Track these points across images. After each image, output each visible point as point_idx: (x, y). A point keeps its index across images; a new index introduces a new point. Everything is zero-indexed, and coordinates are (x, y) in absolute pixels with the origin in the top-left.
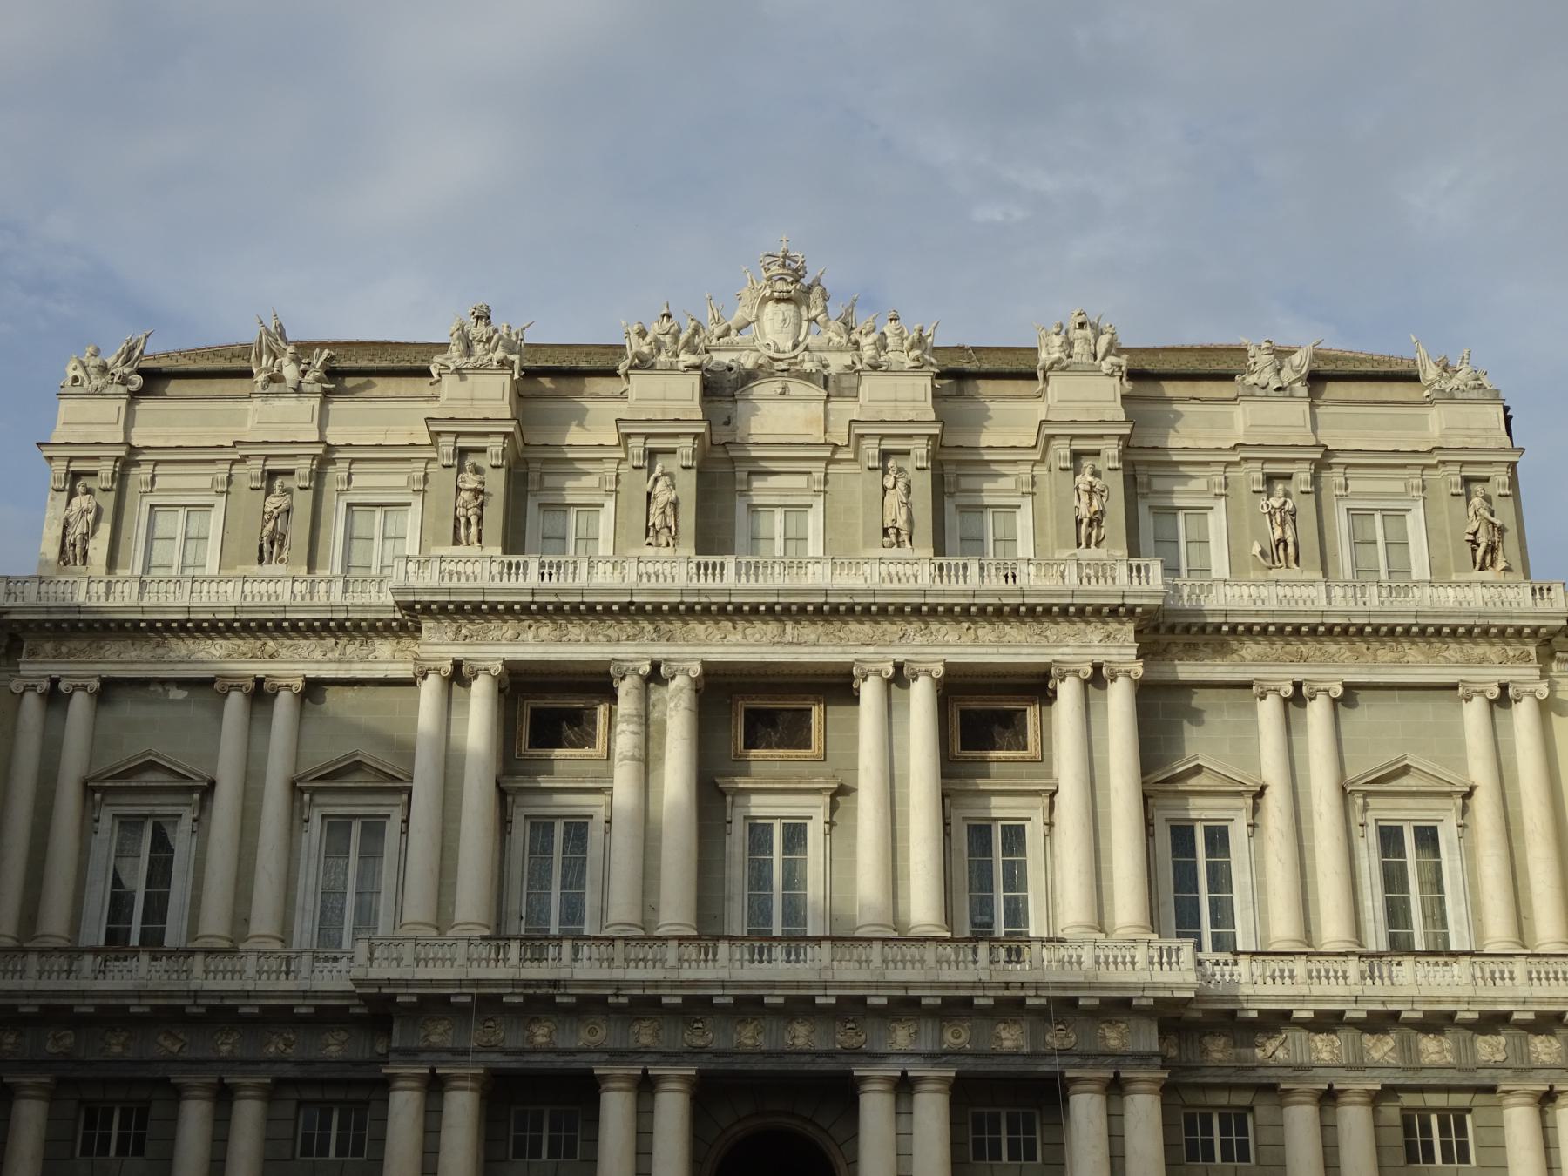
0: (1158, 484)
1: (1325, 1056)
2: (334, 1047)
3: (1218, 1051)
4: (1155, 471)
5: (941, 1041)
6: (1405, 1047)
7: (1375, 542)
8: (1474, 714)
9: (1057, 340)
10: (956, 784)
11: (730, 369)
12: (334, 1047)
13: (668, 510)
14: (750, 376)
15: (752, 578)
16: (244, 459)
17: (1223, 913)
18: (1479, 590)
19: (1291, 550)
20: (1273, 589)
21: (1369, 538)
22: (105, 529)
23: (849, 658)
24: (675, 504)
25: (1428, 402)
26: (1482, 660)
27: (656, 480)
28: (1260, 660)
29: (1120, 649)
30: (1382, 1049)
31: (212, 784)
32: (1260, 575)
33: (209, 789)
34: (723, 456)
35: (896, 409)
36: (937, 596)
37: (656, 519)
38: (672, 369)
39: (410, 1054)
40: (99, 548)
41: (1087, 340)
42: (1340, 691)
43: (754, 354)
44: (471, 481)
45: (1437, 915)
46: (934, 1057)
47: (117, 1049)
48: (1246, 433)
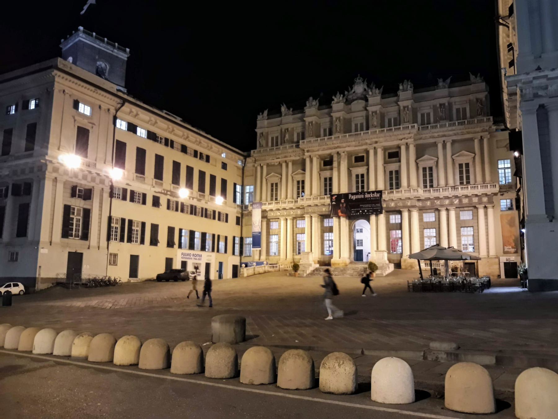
2: (299, 212)
3: (428, 203)
6: (460, 201)
8: (476, 142)
12: (299, 212)
17: (431, 181)
26: (478, 132)
29: (410, 141)
30: (456, 201)
33: (281, 179)
39: (307, 213)
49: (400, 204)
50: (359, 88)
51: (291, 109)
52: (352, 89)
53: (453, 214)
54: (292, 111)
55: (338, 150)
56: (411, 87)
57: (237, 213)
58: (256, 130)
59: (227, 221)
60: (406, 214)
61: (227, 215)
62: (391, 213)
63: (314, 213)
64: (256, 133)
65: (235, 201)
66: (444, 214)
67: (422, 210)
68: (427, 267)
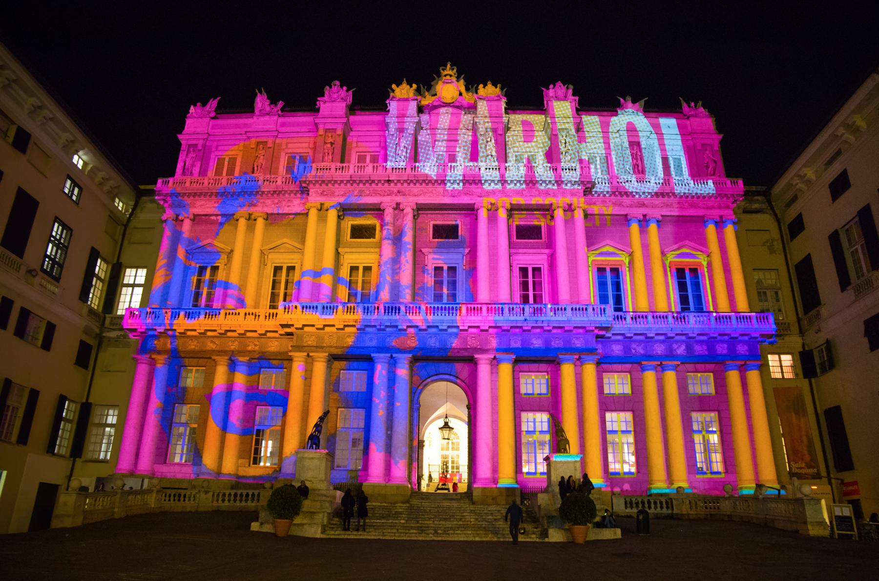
1: (659, 352)
5: (510, 345)
6: (689, 348)
10: (514, 251)
16: (249, 138)
19: (640, 168)
22: (198, 164)
23: (472, 202)
25: (688, 118)
26: (712, 208)
28: (631, 206)
31: (232, 251)
40: (196, 171)
42: (660, 218)
44: (330, 140)
45: (698, 298)
46: (508, 351)
47: (193, 347)
49: (556, 343)
50: (449, 88)
51: (280, 104)
52: (428, 90)
53: (670, 377)
54: (282, 110)
55: (399, 199)
56: (574, 95)
57: (87, 331)
58: (180, 137)
59: (47, 345)
60: (567, 371)
61: (51, 328)
62: (525, 366)
63: (319, 348)
64: (180, 144)
65: (84, 294)
66: (650, 377)
67: (604, 364)
68: (628, 510)
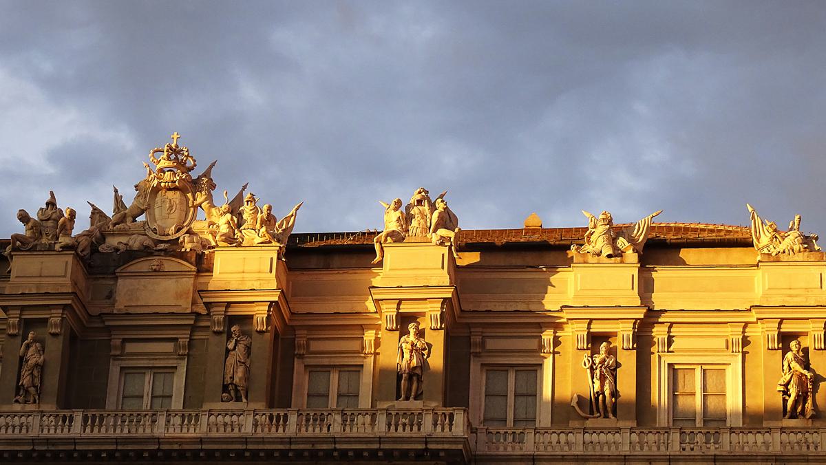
0: (491, 344)
4: (489, 332)
7: (693, 394)
9: (394, 215)
11: (117, 250)
13: (36, 373)
14: (131, 255)
15: (96, 429)
18: (777, 435)
20: (580, 436)
21: (688, 390)
24: (41, 367)
27: (28, 346)
32: (574, 424)
34: (101, 325)
35: (253, 285)
36: (258, 443)
37: (26, 381)
38: (50, 248)
41: (423, 215)
43: (141, 237)
48: (576, 296)
